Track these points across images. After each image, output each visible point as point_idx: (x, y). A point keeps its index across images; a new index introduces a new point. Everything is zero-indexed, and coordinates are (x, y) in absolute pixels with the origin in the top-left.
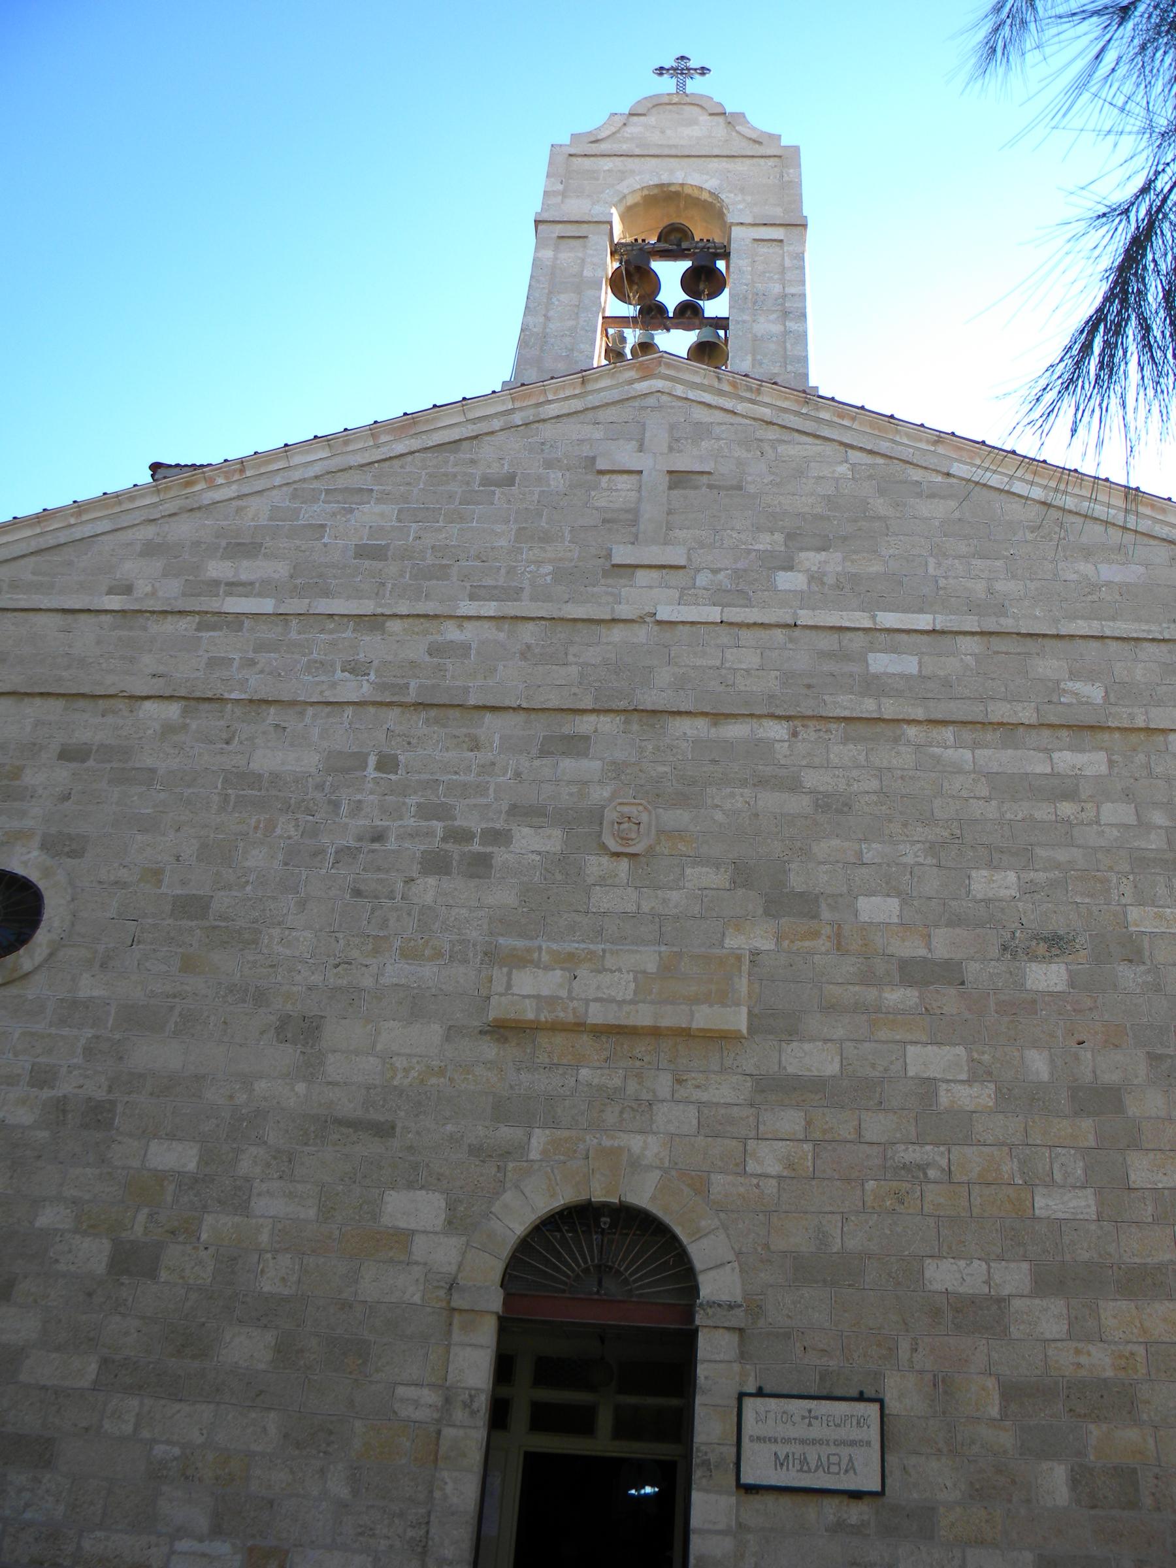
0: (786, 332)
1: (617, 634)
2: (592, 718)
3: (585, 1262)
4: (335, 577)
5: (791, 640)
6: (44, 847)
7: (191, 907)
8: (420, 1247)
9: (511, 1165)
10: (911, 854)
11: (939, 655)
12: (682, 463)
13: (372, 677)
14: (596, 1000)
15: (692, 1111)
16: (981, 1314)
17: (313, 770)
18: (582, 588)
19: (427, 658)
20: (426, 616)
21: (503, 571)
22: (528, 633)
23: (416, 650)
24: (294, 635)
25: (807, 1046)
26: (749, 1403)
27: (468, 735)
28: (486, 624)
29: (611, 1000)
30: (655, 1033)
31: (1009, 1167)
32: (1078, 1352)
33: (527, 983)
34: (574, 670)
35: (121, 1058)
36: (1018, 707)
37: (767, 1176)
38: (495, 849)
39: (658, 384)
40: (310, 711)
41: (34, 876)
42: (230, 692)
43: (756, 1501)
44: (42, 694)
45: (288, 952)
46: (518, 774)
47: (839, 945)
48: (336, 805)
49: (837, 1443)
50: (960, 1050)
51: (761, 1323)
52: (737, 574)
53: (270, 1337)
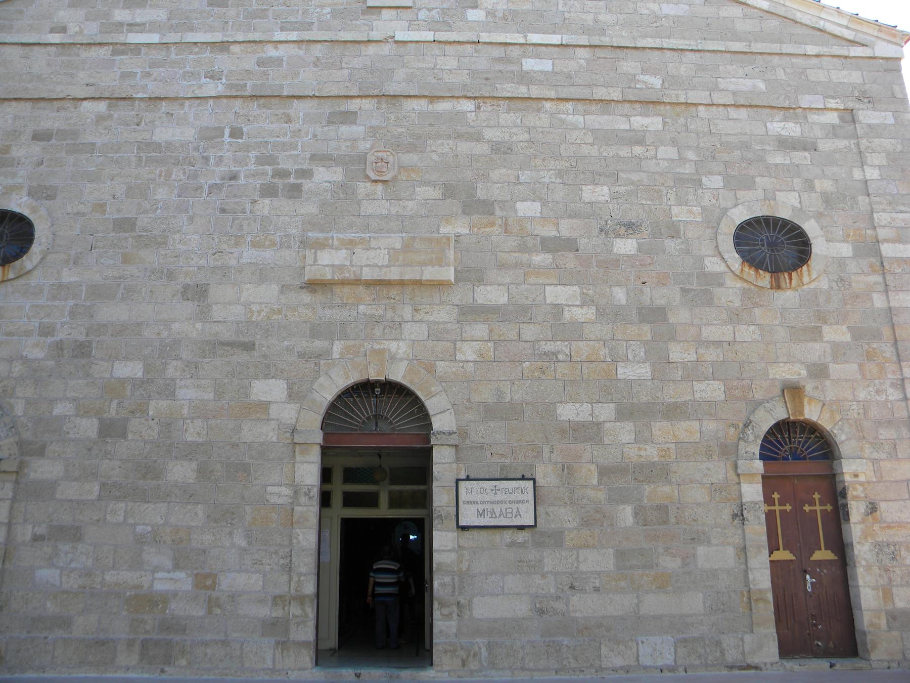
1: (371, 49)
2: (358, 101)
3: (368, 413)
4: (196, 19)
5: (476, 51)
6: (30, 194)
7: (125, 225)
8: (274, 411)
9: (322, 362)
10: (547, 177)
11: (565, 59)
13: (224, 81)
14: (366, 266)
15: (424, 327)
16: (588, 432)
17: (192, 139)
18: (349, 22)
19: (257, 68)
20: (254, 42)
21: (300, 12)
22: (317, 51)
23: (250, 63)
24: (173, 56)
25: (488, 288)
26: (462, 484)
27: (284, 114)
28: (292, 46)
29: (375, 266)
30: (401, 283)
31: (603, 352)
32: (639, 449)
33: (326, 258)
34: (346, 72)
35: (92, 316)
36: (611, 90)
37: (468, 361)
38: (303, 181)
40: (187, 103)
41: (26, 213)
42: (136, 93)
43: (467, 534)
44: (15, 99)
45: (185, 248)
46: (315, 136)
47: (507, 231)
48: (207, 159)
49: (511, 502)
50: (576, 288)
51: (467, 441)
52: (443, 12)
53: (194, 465)
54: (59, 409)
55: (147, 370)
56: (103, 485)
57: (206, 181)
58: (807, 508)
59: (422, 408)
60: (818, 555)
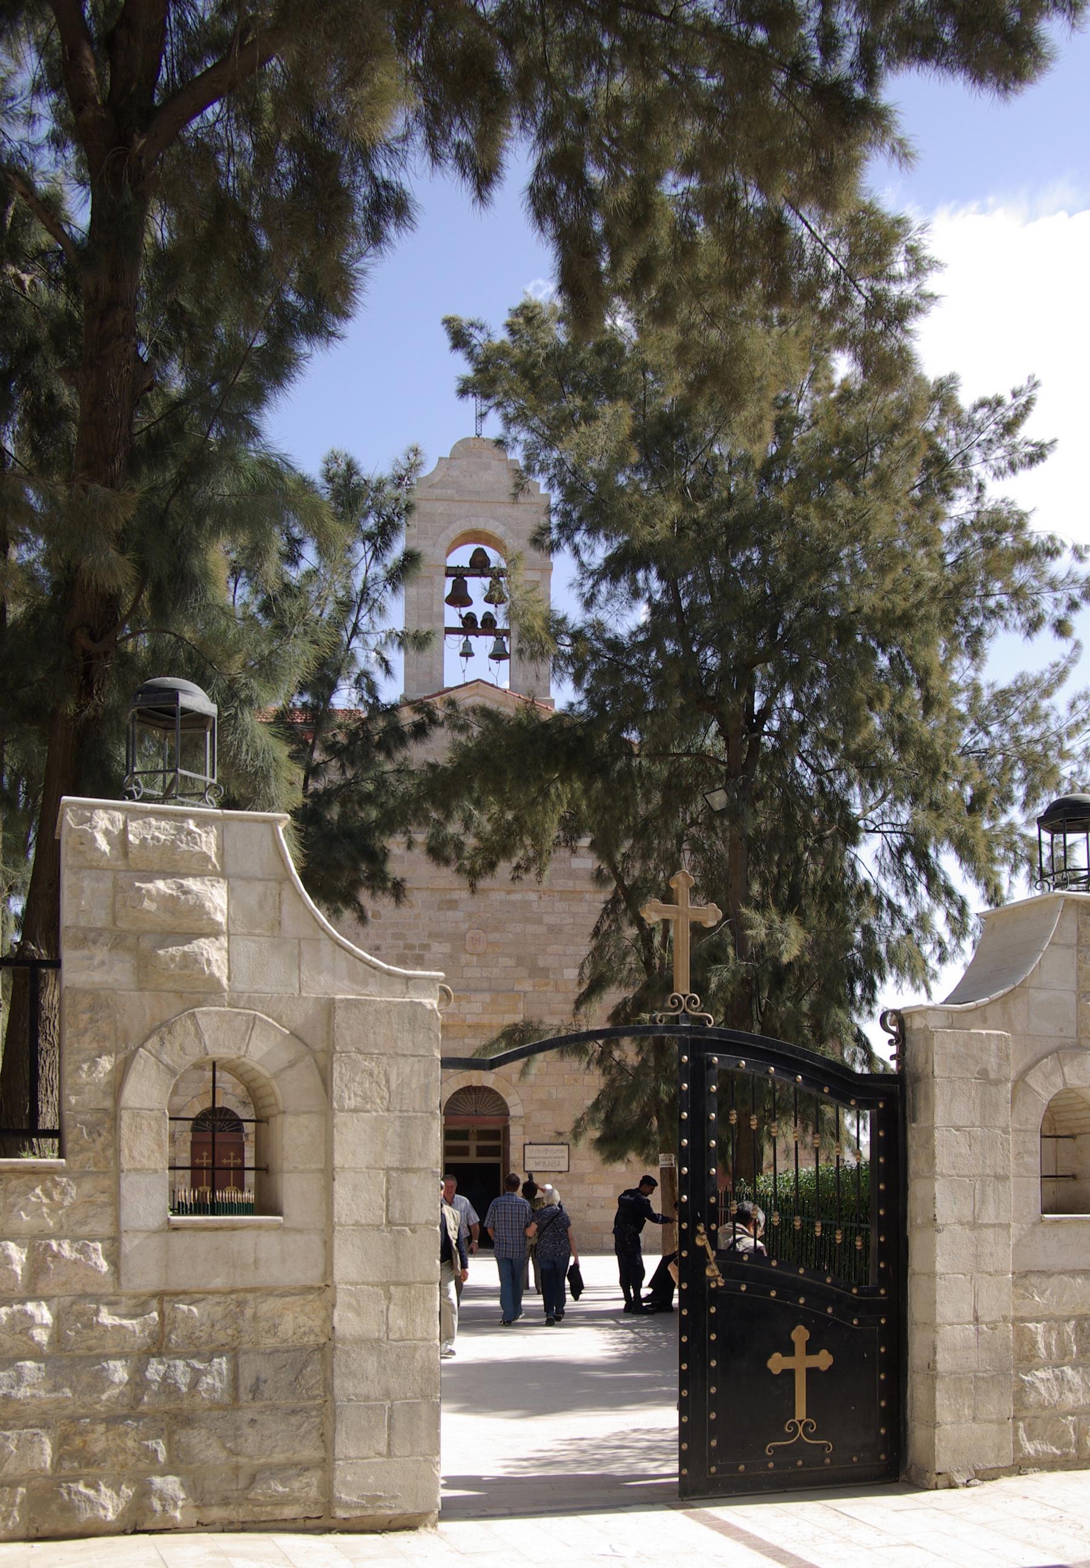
59: (504, 1103)
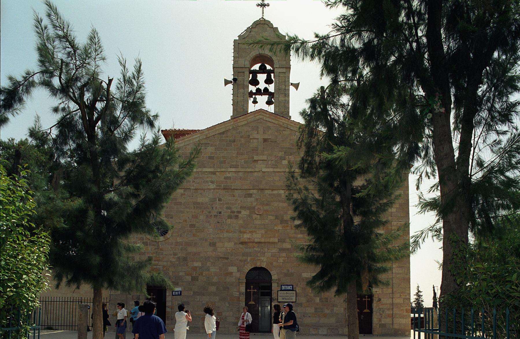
0: (285, 100)
1: (255, 174)
8: (234, 274)
12: (266, 137)
22: (241, 174)
30: (265, 243)
39: (261, 117)
54: (181, 274)
55: (202, 264)
56: (194, 292)
57: (213, 214)
58: (364, 299)
60: (365, 311)
